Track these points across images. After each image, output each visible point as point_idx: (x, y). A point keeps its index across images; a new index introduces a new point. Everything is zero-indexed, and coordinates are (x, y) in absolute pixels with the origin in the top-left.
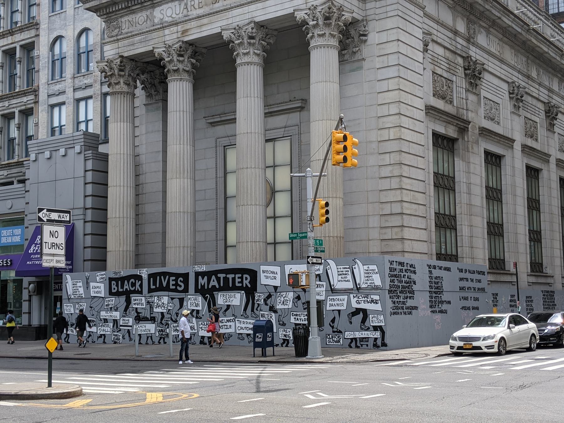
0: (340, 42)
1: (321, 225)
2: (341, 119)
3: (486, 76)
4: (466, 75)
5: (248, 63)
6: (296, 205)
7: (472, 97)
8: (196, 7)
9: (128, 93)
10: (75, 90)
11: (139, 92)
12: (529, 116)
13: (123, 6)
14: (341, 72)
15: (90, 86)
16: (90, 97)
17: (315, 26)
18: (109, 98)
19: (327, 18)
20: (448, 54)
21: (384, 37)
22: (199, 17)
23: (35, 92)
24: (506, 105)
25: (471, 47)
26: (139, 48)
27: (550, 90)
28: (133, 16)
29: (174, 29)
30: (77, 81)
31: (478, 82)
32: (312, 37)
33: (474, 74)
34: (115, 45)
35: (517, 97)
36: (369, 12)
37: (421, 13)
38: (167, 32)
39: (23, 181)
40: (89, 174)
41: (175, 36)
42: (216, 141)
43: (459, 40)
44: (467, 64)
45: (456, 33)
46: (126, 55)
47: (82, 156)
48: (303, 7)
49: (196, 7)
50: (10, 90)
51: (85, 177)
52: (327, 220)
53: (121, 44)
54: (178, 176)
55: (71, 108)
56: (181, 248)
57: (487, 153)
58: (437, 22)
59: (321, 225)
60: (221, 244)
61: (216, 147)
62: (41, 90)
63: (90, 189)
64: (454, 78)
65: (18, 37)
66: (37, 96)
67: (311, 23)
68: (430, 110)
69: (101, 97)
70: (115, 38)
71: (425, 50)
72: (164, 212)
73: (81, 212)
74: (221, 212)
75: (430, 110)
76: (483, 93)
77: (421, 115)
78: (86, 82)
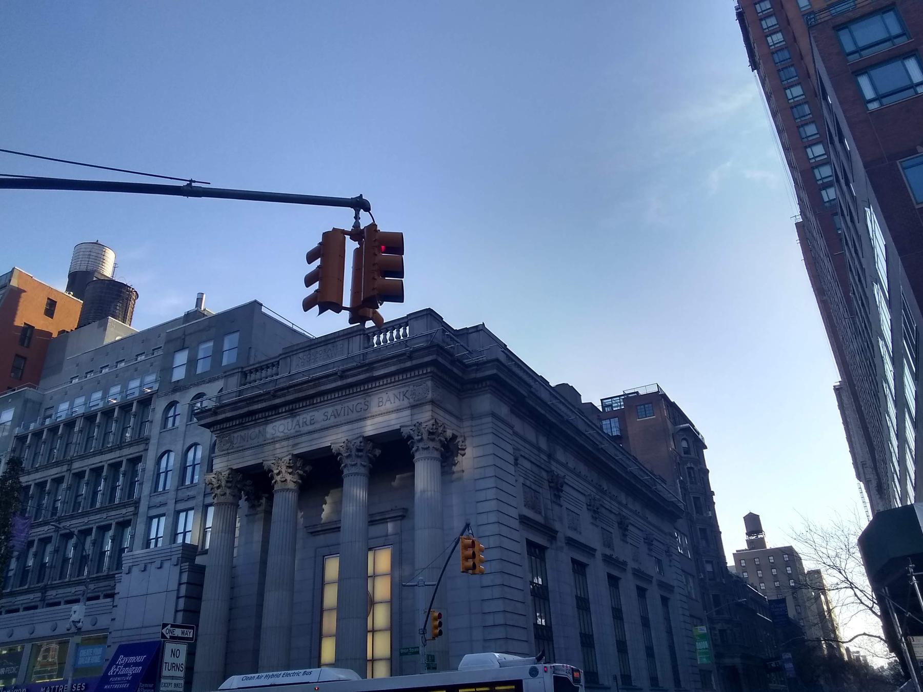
0: (442, 455)
1: (434, 638)
2: (467, 526)
3: (566, 488)
4: (550, 487)
7: (556, 508)
8: (308, 423)
9: (232, 504)
11: (243, 503)
12: (605, 526)
17: (421, 440)
18: (211, 511)
19: (430, 433)
20: (535, 469)
22: (310, 433)
23: (137, 504)
24: (585, 516)
25: (552, 462)
26: (248, 460)
27: (620, 503)
28: (246, 432)
29: (285, 443)
30: (180, 493)
31: (561, 494)
32: (417, 450)
33: (557, 487)
34: (225, 459)
35: (595, 511)
37: (511, 432)
38: (277, 446)
39: (112, 596)
40: (183, 587)
41: (285, 449)
43: (543, 456)
45: (539, 449)
46: (235, 467)
47: (178, 569)
48: (409, 423)
49: (308, 423)
51: (178, 590)
52: (441, 633)
53: (230, 457)
55: (171, 519)
57: (574, 561)
58: (525, 440)
59: (434, 638)
62: (142, 502)
64: (540, 490)
66: (137, 508)
67: (416, 438)
68: (524, 520)
71: (516, 464)
72: (258, 627)
75: (524, 520)
76: (565, 505)
77: (515, 524)
78: (189, 493)
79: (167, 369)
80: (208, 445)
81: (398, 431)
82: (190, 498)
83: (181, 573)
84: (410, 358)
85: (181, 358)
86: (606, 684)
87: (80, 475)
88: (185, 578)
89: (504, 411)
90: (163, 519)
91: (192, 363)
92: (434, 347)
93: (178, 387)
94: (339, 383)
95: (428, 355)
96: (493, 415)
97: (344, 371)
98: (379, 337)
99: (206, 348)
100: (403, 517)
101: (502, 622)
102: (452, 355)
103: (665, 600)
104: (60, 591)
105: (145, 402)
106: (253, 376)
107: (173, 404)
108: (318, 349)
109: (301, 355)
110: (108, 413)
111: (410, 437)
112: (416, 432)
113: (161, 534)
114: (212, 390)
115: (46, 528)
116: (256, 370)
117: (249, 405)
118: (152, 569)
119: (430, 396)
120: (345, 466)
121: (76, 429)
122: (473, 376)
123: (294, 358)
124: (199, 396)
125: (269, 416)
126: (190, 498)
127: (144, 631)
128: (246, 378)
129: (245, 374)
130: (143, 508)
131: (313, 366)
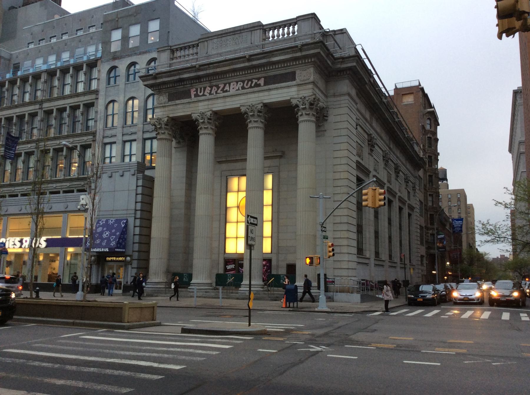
4: (369, 144)
5: (257, 127)
10: (123, 135)
14: (317, 136)
16: (135, 140)
17: (304, 109)
19: (311, 104)
21: (338, 118)
30: (125, 129)
34: (162, 109)
36: (329, 104)
44: (370, 138)
47: (135, 177)
50: (73, 132)
51: (136, 190)
53: (166, 109)
62: (98, 133)
63: (139, 198)
65: (82, 98)
73: (133, 212)
77: (354, 165)
79: (107, 43)
80: (143, 99)
81: (289, 101)
83: (137, 179)
84: (301, 50)
85: (117, 35)
86: (383, 259)
87: (49, 113)
88: (140, 183)
89: (353, 92)
90: (114, 146)
91: (125, 39)
92: (321, 44)
93: (116, 57)
94: (247, 64)
95: (314, 49)
96: (349, 94)
97: (251, 56)
98: (273, 32)
99: (135, 30)
100: (281, 157)
101: (346, 221)
102: (328, 50)
103: (410, 215)
104: (58, 185)
105: (92, 65)
106: (178, 54)
107: (114, 68)
108: (228, 37)
109: (215, 40)
110: (65, 71)
111: (297, 106)
112: (301, 103)
113: (114, 154)
114: (142, 61)
115: (29, 146)
116: (181, 49)
117: (179, 74)
118: (117, 176)
119: (312, 79)
120: (250, 122)
121: (42, 80)
122: (339, 66)
123: (210, 42)
124: (133, 64)
125: (194, 83)
127: (114, 213)
128: (173, 54)
129: (173, 51)
130: (99, 137)
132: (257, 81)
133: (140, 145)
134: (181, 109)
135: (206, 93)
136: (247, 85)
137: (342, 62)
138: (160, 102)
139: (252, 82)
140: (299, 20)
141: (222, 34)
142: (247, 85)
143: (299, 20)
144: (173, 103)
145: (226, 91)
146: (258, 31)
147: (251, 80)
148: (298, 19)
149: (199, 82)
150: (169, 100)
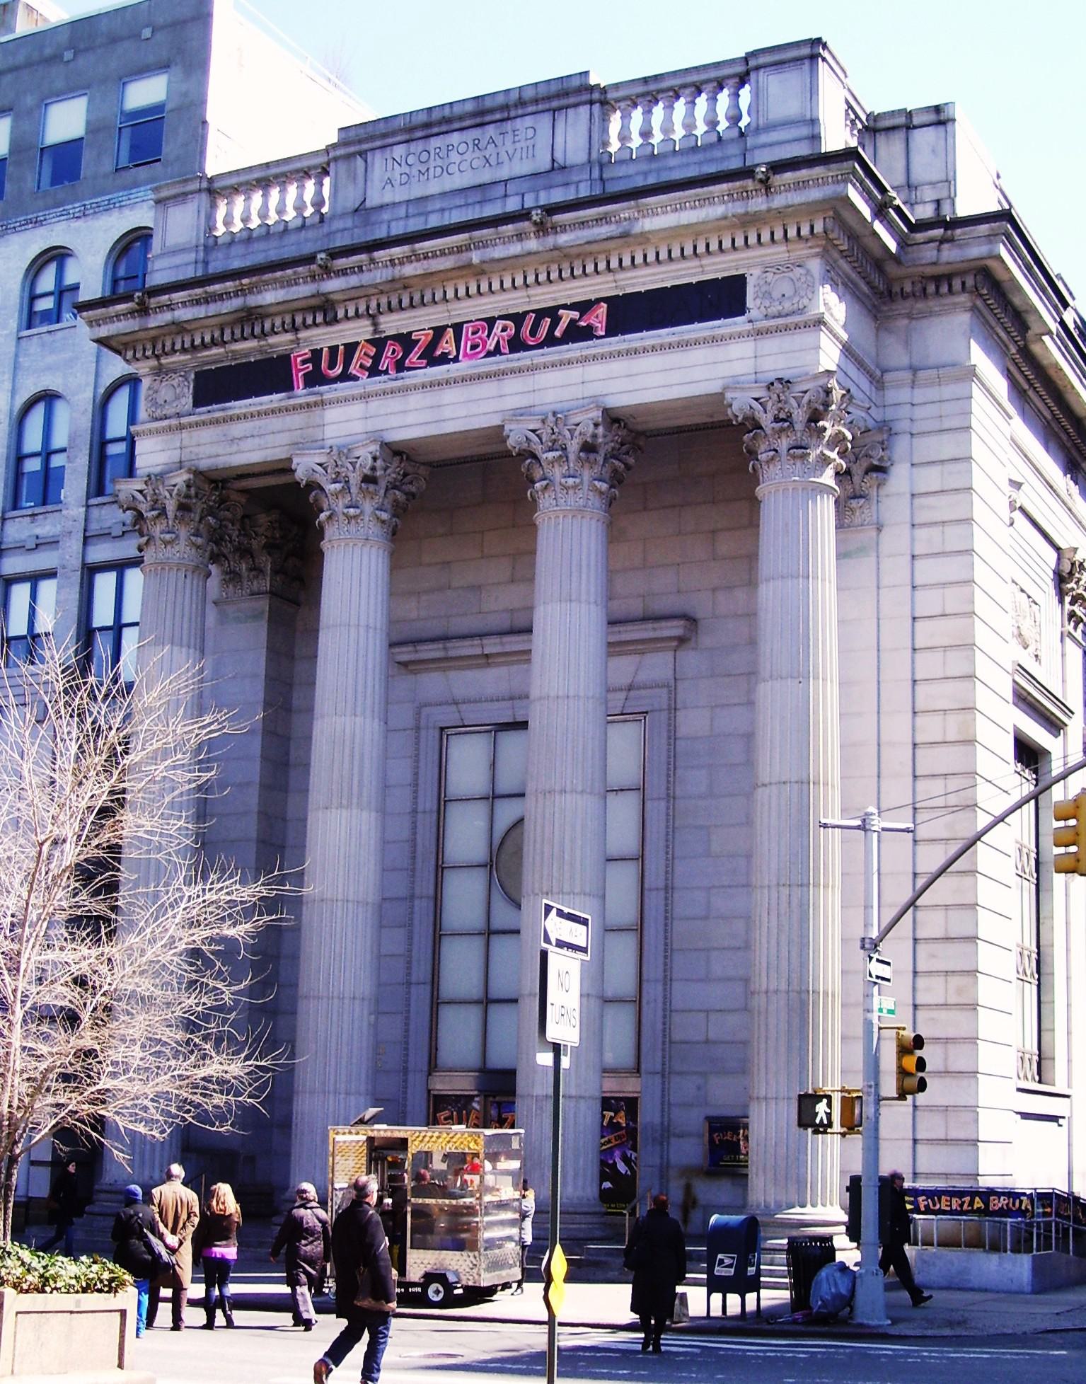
6: (655, 901)
13: (208, 339)
15: (53, 543)
16: (51, 574)
34: (175, 439)
36: (890, 414)
42: (419, 713)
54: (344, 802)
56: (346, 1001)
60: (421, 996)
61: (418, 728)
69: (82, 573)
70: (174, 422)
74: (423, 907)
78: (38, 531)
82: (40, 544)
97: (551, 210)
100: (682, 640)
108: (455, 138)
109: (399, 151)
123: (378, 160)
124: (57, 256)
126: (40, 544)
131: (434, 188)
132: (576, 315)
133: (74, 595)
134: (250, 436)
135: (353, 370)
136: (533, 333)
137: (942, 241)
138: (158, 413)
139: (556, 320)
140: (757, 68)
141: (427, 125)
142: (533, 333)
143: (757, 68)
144: (217, 411)
145: (444, 359)
146: (584, 110)
147: (552, 313)
148: (752, 63)
149: (327, 323)
150: (197, 403)
